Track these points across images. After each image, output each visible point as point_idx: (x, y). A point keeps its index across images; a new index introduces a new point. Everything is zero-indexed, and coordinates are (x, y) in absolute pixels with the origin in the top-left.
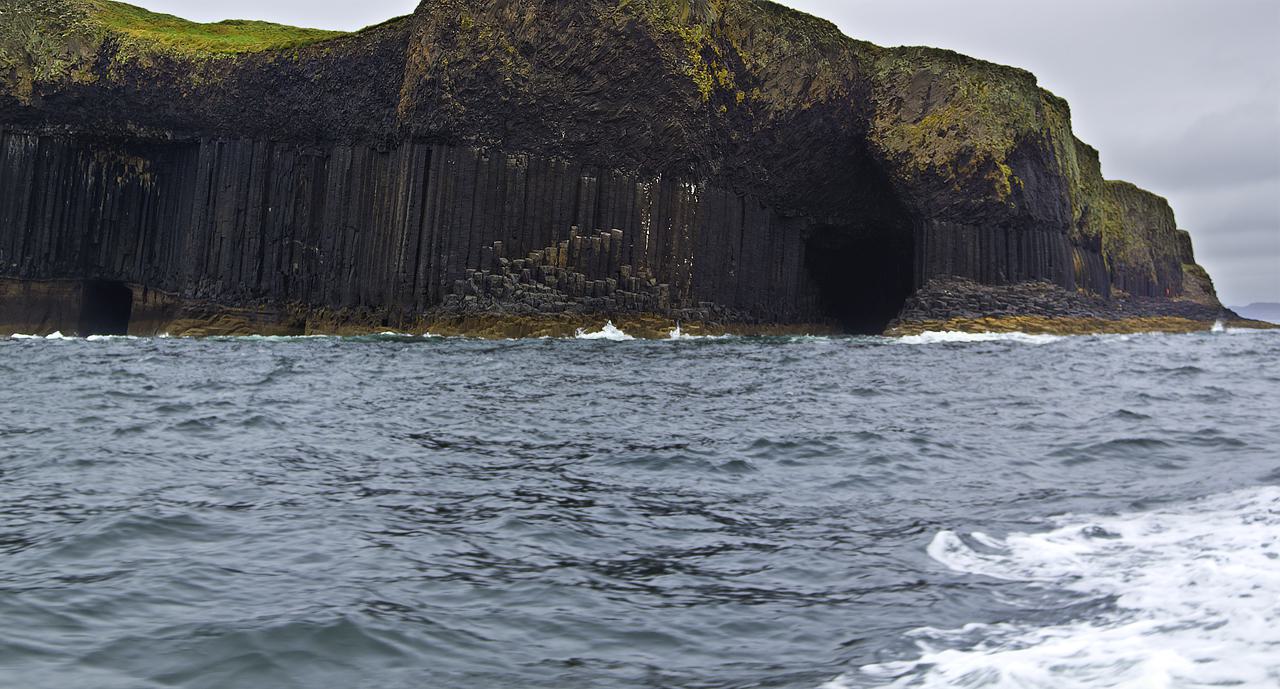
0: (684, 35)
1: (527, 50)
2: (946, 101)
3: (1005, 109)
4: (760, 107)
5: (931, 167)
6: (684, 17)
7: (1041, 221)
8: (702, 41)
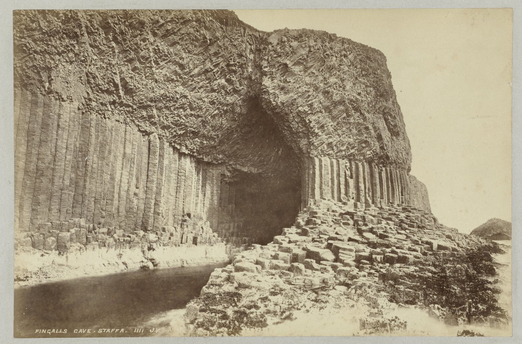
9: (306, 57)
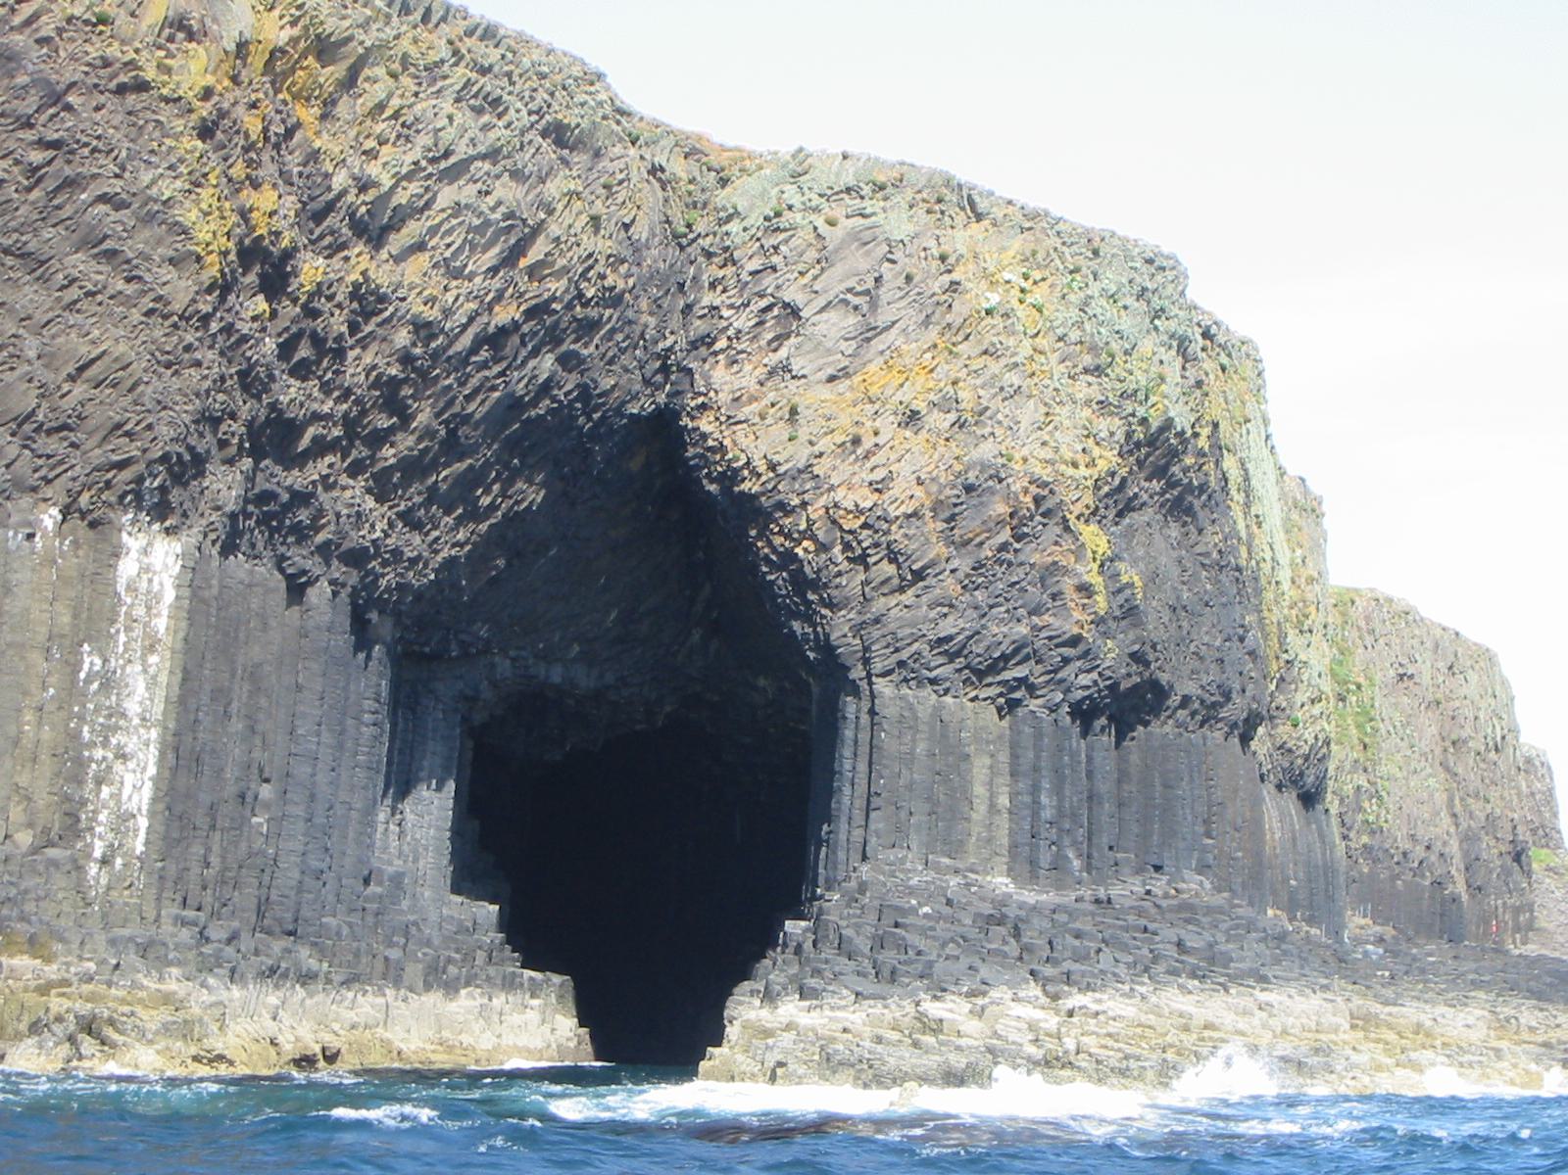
0: (150, 74)
2: (927, 322)
3: (1098, 356)
7: (1186, 701)
8: (207, 94)
9: (870, 284)
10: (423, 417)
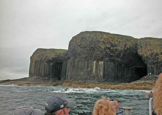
0: (99, 40)
1: (79, 46)
4: (116, 50)
5: (147, 56)
6: (100, 37)
10: (122, 55)
